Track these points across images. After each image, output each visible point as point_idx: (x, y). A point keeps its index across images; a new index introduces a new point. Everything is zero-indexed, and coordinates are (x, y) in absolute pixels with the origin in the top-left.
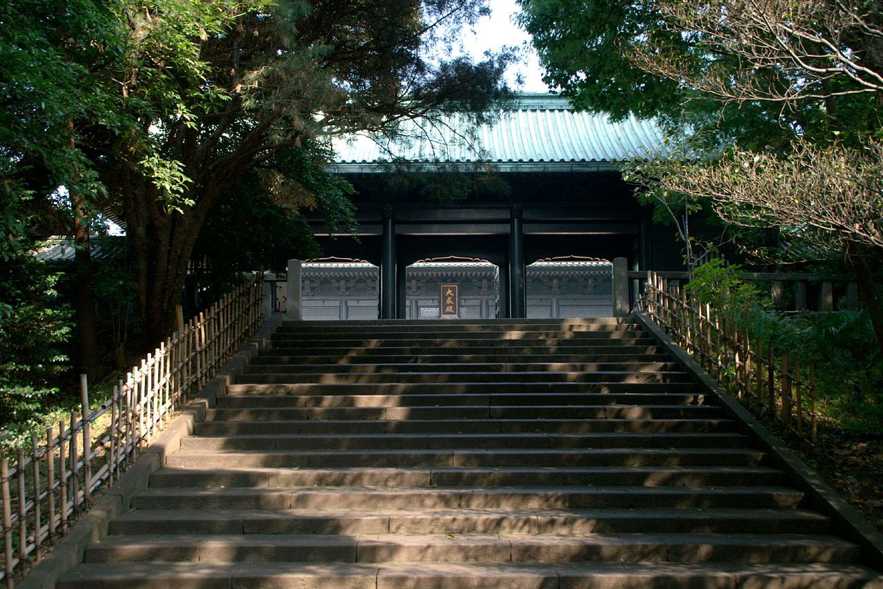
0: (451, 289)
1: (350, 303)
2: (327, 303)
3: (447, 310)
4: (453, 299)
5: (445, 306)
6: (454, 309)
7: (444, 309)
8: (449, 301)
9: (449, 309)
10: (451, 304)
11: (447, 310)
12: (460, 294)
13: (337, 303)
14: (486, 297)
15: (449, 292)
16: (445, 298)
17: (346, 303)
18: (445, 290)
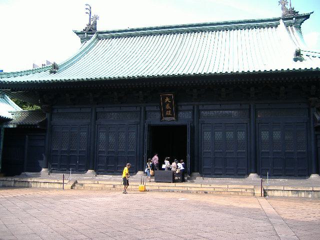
0: (169, 97)
1: (98, 110)
2: (83, 110)
3: (167, 114)
4: (171, 105)
5: (165, 110)
6: (172, 113)
7: (165, 114)
8: (168, 107)
9: (168, 113)
10: (168, 110)
11: (167, 114)
12: (176, 103)
13: (89, 110)
14: (197, 103)
15: (167, 100)
16: (165, 104)
17: (96, 110)
18: (164, 98)
